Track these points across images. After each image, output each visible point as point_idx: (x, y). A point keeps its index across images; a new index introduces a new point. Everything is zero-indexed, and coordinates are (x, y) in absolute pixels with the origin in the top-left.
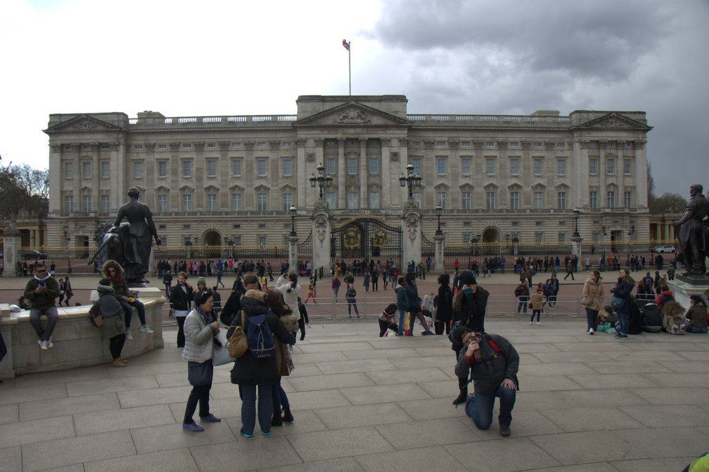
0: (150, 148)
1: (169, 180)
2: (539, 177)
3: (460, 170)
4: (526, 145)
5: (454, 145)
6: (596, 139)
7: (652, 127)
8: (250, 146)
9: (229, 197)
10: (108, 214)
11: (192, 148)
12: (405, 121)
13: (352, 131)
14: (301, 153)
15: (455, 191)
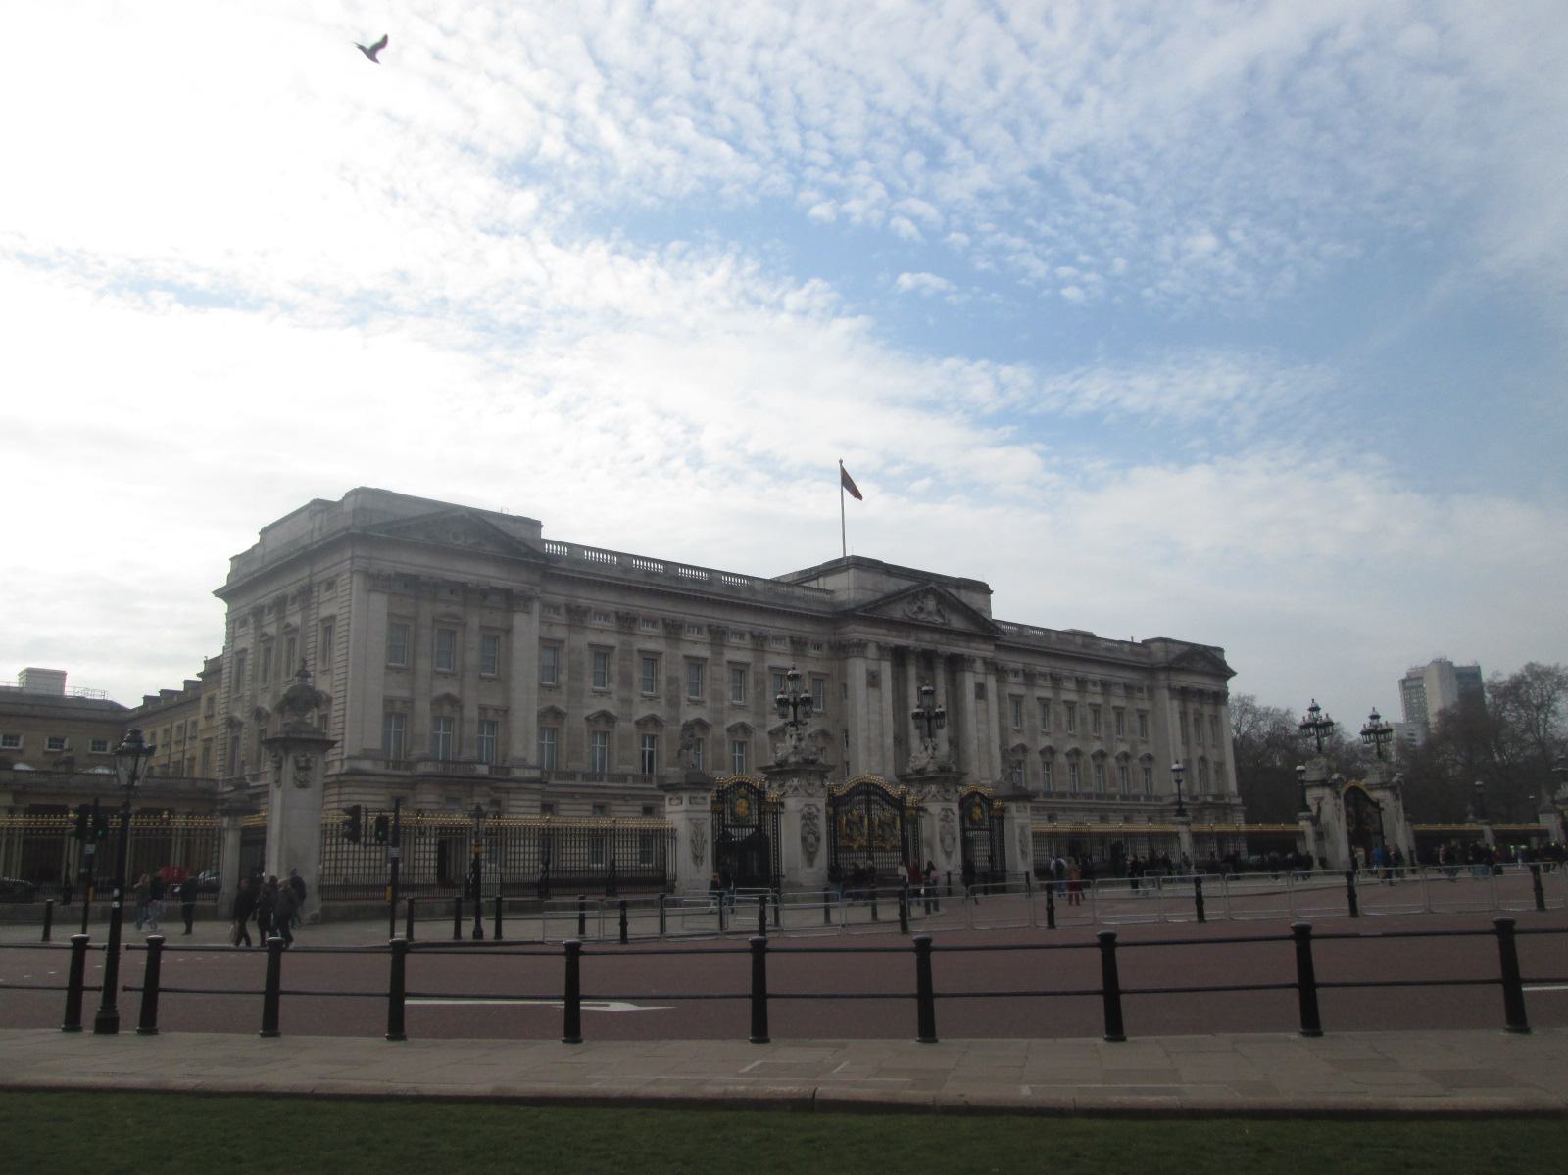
0: (577, 616)
1: (615, 697)
2: (1122, 741)
3: (1038, 722)
4: (1106, 686)
5: (1030, 678)
6: (1184, 685)
7: (1233, 673)
8: (759, 641)
9: (727, 747)
10: (507, 770)
11: (659, 631)
12: (997, 628)
13: (927, 636)
14: (858, 669)
15: (1034, 759)
